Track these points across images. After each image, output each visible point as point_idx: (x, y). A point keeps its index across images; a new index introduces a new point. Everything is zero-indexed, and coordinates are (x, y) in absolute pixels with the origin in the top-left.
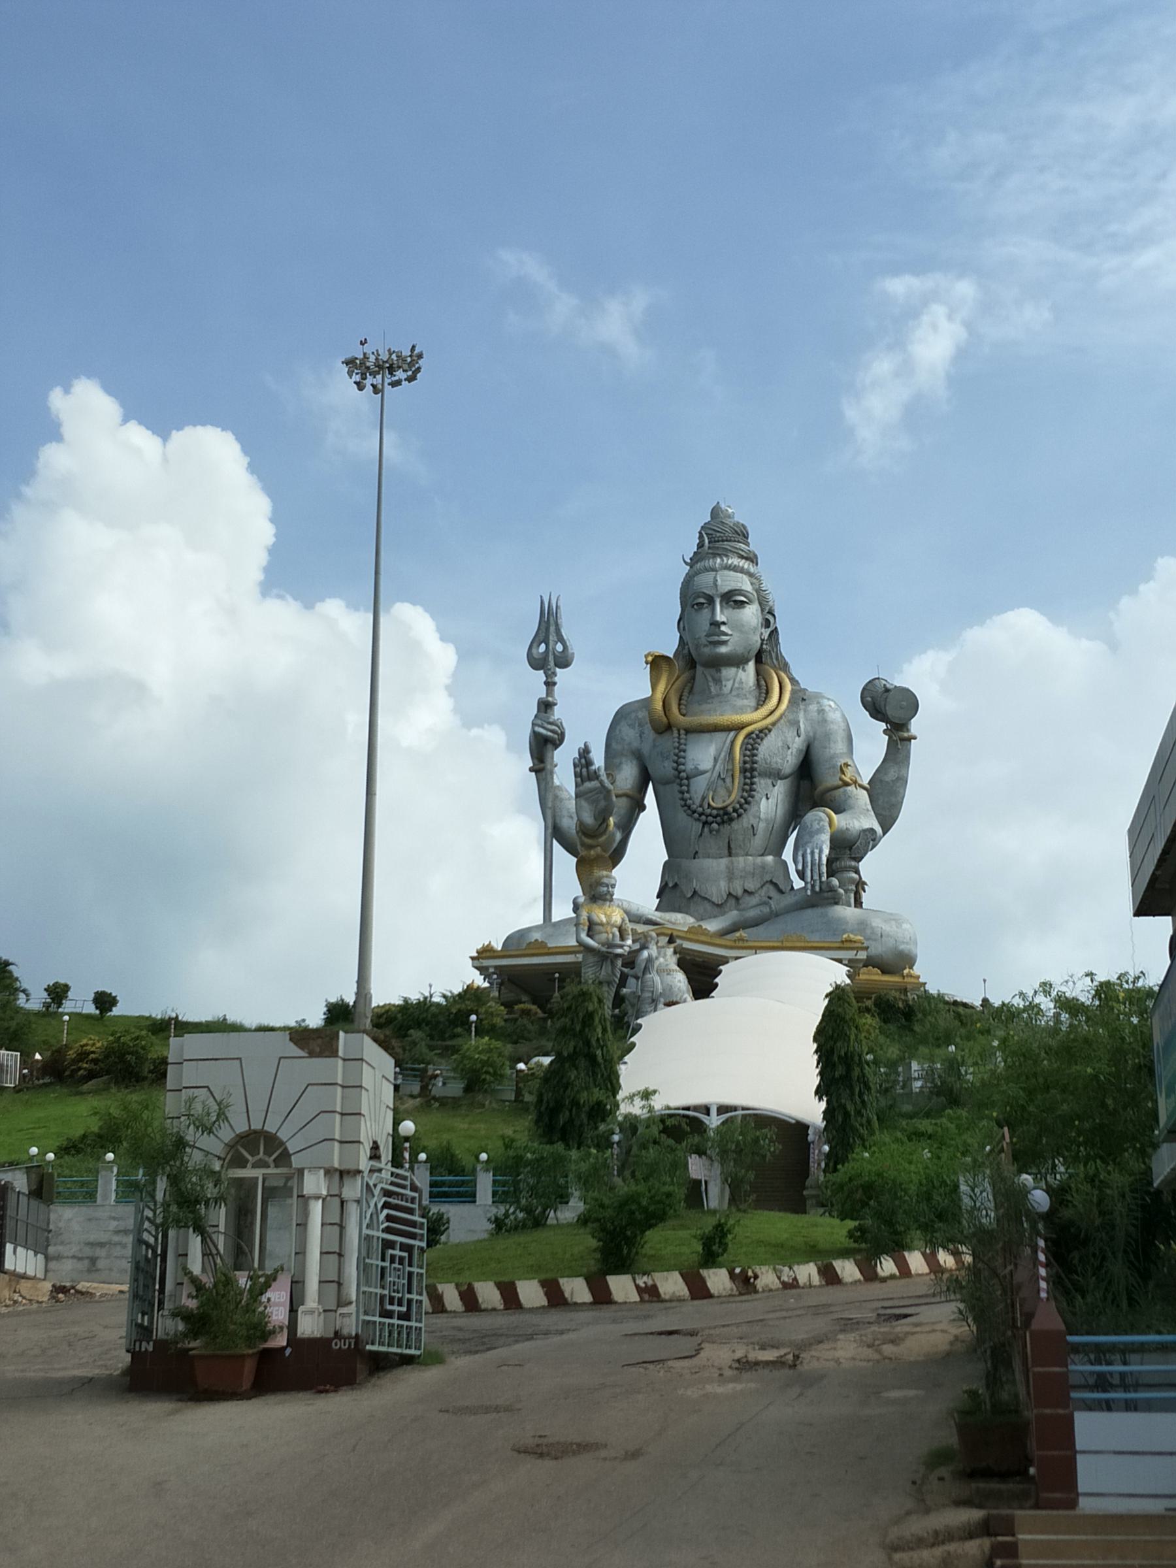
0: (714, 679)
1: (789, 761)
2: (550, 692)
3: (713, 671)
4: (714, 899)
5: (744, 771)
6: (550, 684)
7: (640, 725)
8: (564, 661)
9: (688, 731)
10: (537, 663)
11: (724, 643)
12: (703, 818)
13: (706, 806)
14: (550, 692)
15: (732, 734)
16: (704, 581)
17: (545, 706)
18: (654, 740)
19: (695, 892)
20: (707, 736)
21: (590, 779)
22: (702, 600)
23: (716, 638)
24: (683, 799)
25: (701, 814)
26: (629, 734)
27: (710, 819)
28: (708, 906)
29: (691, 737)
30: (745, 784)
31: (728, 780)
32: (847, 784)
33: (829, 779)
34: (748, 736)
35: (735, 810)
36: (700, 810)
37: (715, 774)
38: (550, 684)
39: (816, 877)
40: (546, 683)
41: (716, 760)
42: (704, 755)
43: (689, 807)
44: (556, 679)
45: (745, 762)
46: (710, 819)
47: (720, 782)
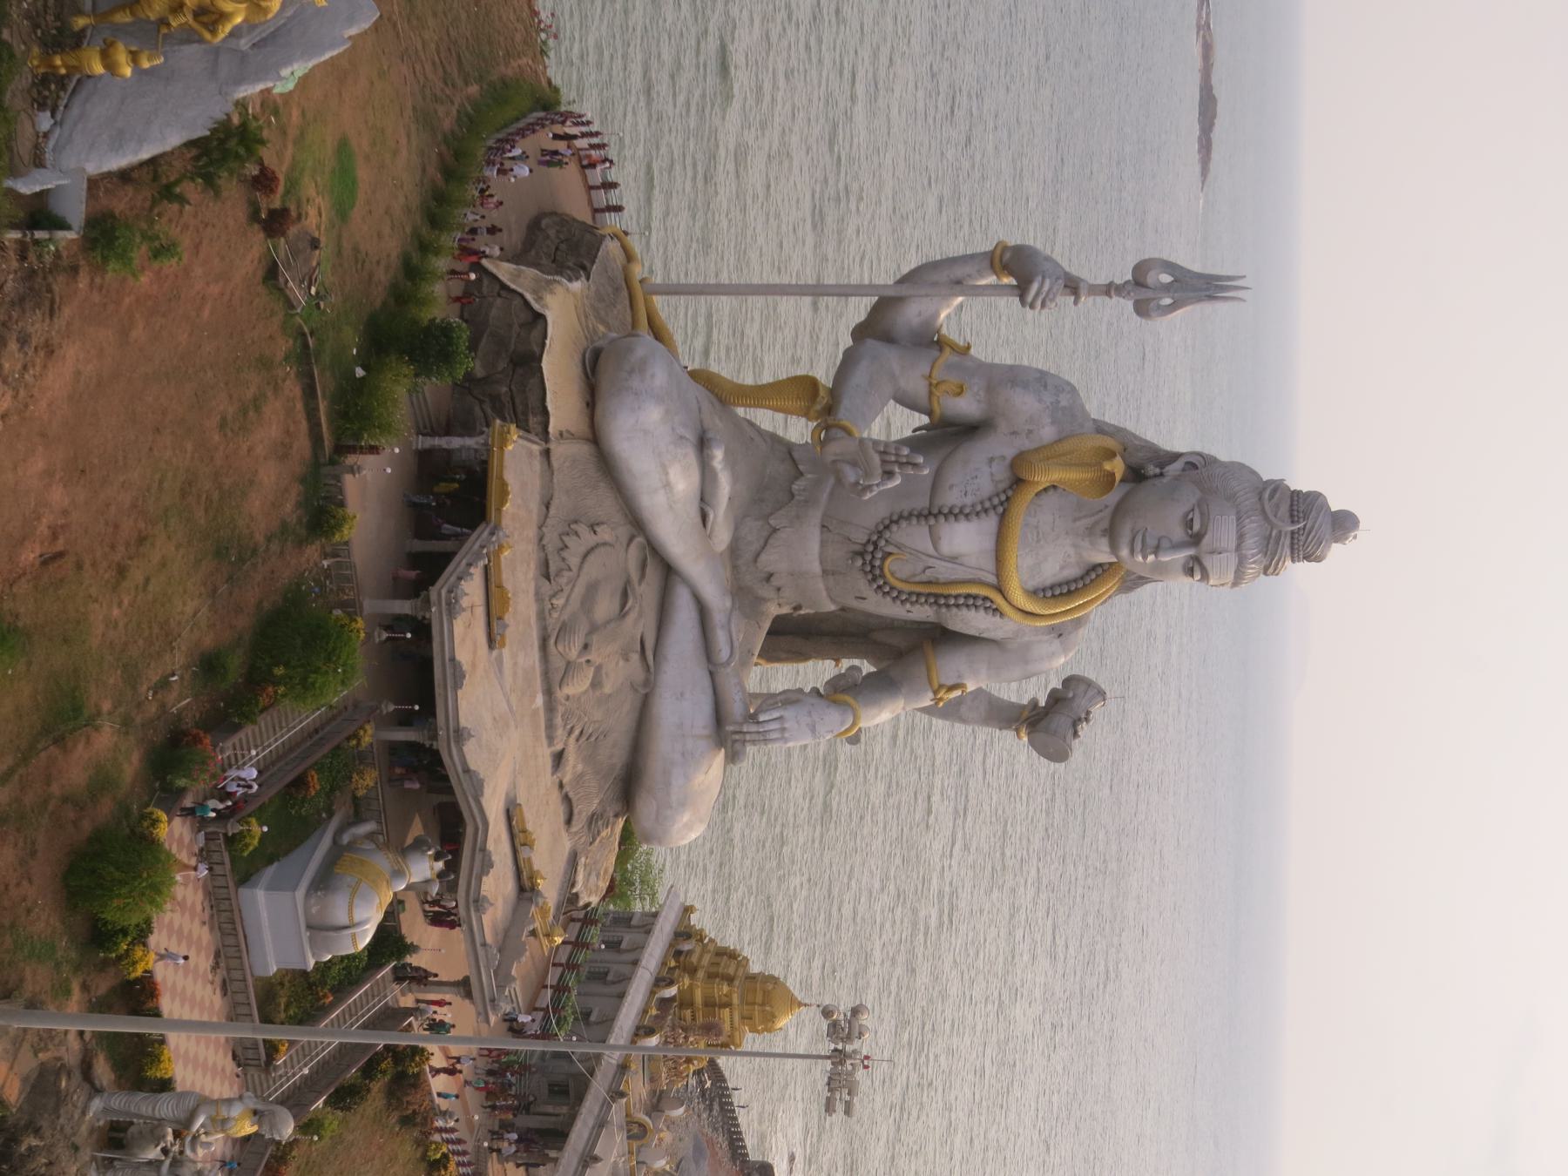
0: (1096, 523)
1: (973, 621)
2: (1095, 290)
3: (1105, 524)
4: (763, 557)
5: (937, 596)
6: (1109, 290)
7: (1030, 432)
8: (1142, 309)
9: (1003, 518)
10: (1141, 269)
11: (1132, 551)
12: (871, 548)
13: (890, 549)
14: (1095, 290)
15: (992, 579)
16: (1223, 531)
17: (1073, 287)
18: (1003, 458)
19: (775, 530)
20: (989, 543)
21: (884, 462)
22: (1196, 527)
23: (1138, 546)
24: (901, 517)
25: (875, 544)
26: (1025, 404)
27: (868, 557)
28: (756, 546)
29: (990, 523)
30: (919, 595)
31: (924, 578)
32: (935, 693)
33: (951, 665)
34: (985, 598)
35: (879, 587)
36: (882, 543)
37: (931, 562)
38: (1109, 290)
39: (748, 737)
40: (1111, 284)
41: (953, 559)
42: (966, 541)
43: (887, 527)
44: (1115, 299)
45: (947, 597)
46: (868, 557)
47: (920, 567)
